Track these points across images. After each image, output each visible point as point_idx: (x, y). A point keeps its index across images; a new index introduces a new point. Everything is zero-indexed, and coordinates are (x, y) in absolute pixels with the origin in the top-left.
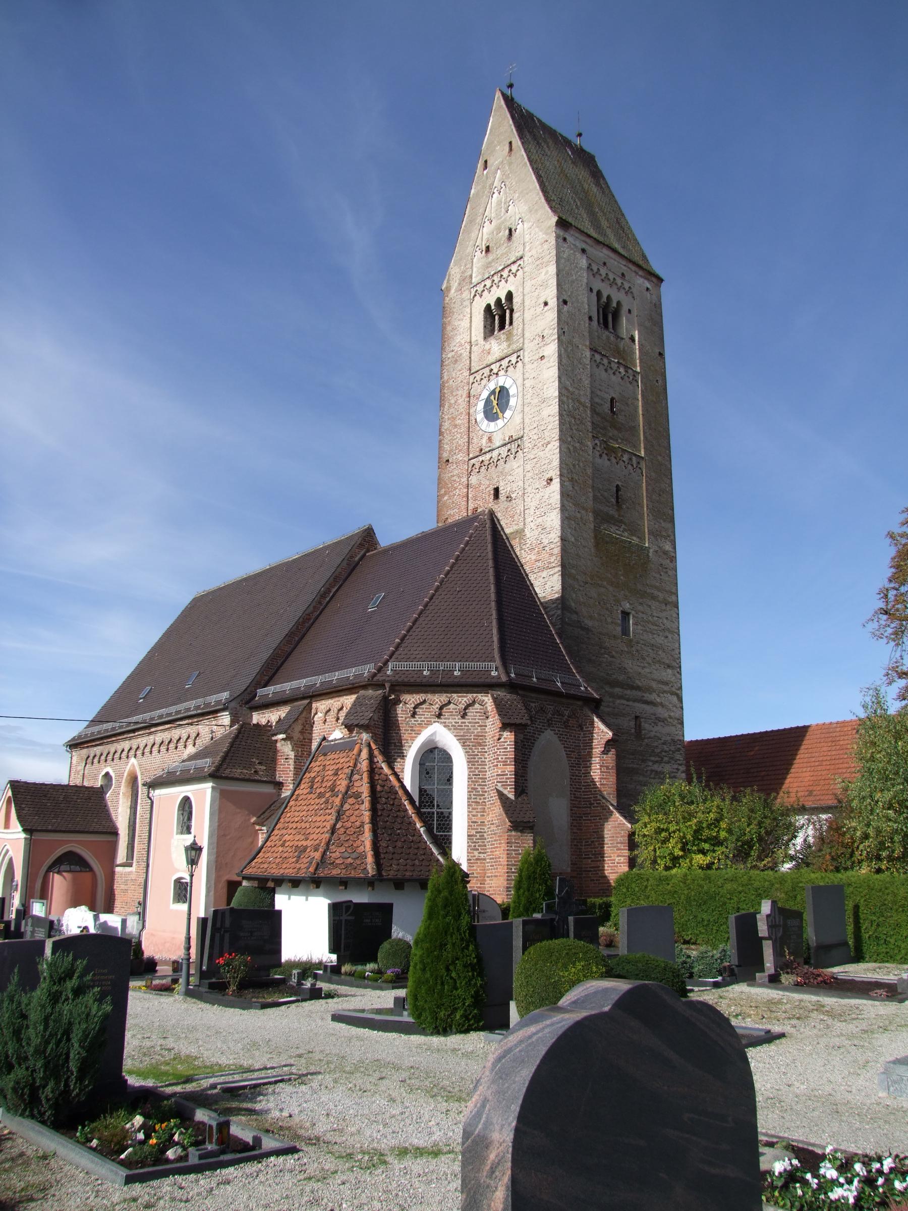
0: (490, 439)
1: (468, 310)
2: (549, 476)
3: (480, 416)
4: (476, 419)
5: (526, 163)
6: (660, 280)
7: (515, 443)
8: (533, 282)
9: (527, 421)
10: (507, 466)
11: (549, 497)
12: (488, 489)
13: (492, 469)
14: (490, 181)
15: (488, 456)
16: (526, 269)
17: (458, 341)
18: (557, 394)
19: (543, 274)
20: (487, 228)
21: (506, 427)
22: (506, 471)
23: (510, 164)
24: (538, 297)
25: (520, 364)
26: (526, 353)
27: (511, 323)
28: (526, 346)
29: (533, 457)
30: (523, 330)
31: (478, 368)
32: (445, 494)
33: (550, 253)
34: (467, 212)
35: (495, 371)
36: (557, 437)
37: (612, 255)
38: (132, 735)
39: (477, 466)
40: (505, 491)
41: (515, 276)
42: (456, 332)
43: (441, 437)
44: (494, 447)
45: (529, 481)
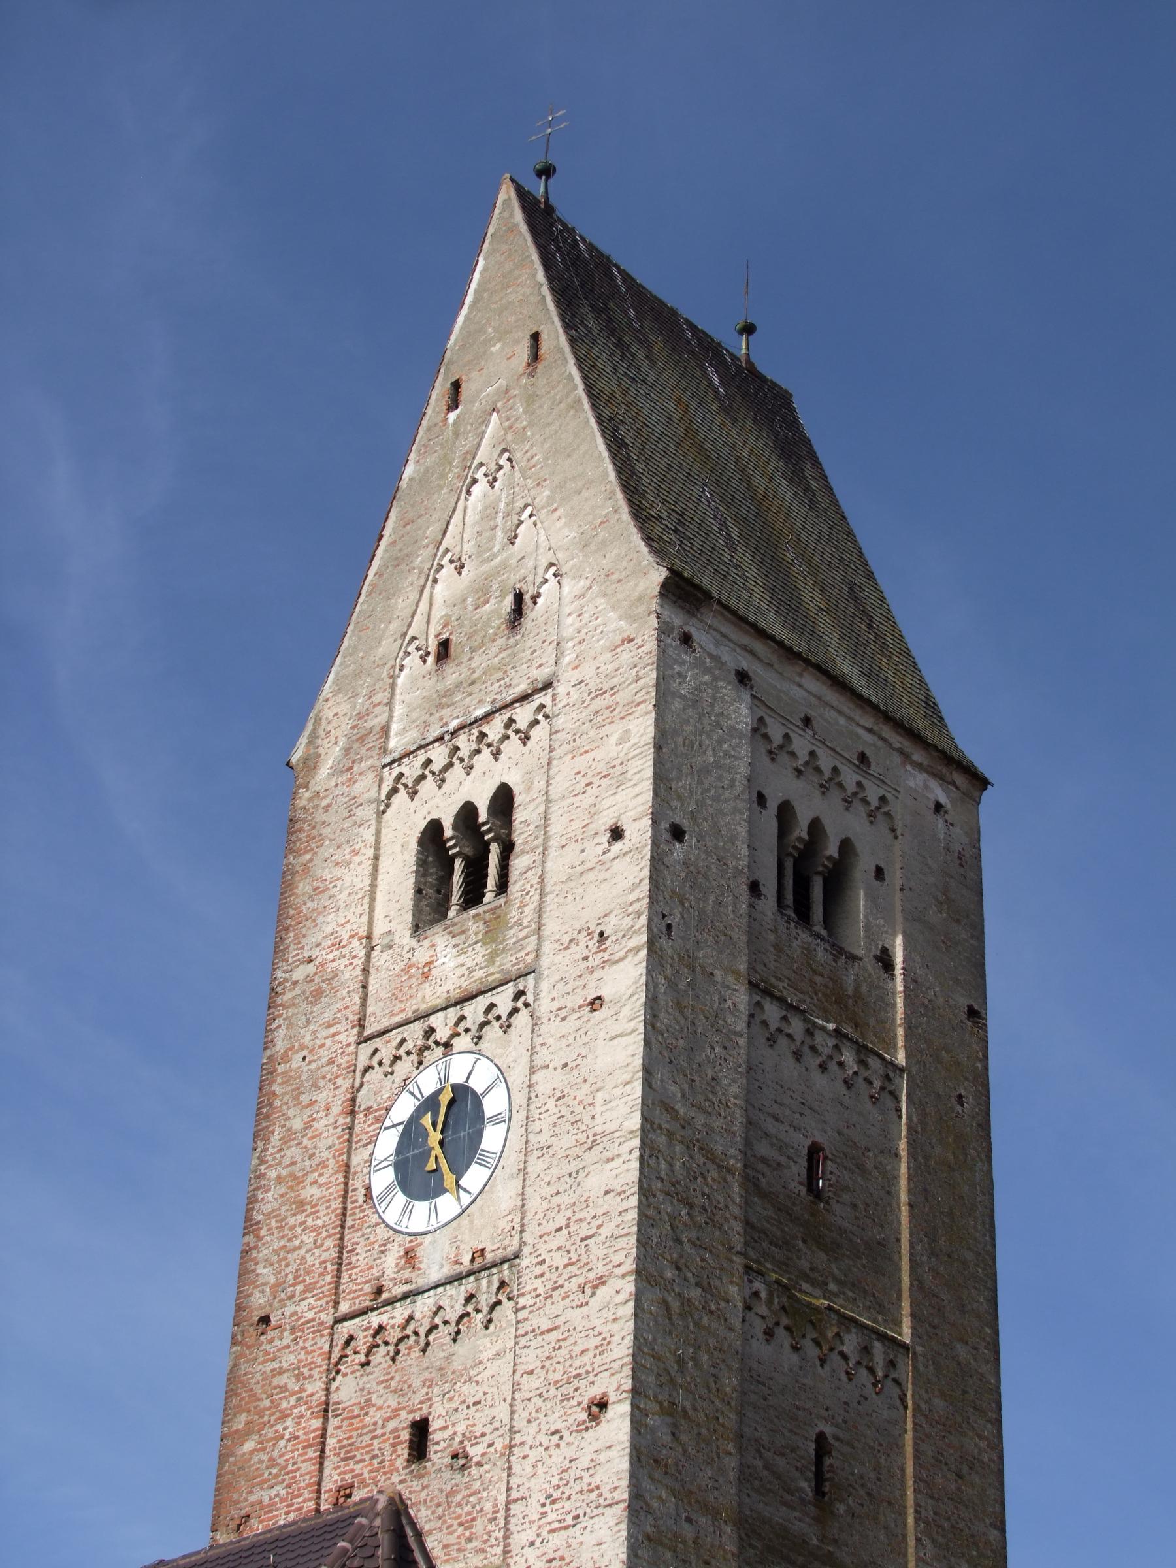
0: (410, 1257)
1: (369, 835)
2: (595, 1392)
3: (383, 1179)
4: (368, 1189)
5: (579, 400)
6: (981, 782)
8: (581, 762)
10: (462, 1349)
11: (594, 1465)
12: (392, 1425)
13: (411, 1357)
14: (464, 445)
15: (399, 1313)
16: (559, 722)
17: (328, 930)
18: (635, 1122)
19: (613, 739)
20: (448, 586)
21: (464, 1221)
22: (456, 1365)
23: (531, 399)
24: (593, 811)
25: (522, 1018)
26: (545, 986)
27: (503, 887)
28: (545, 962)
29: (546, 1324)
30: (540, 910)
31: (386, 1023)
33: (638, 679)
34: (387, 533)
35: (442, 1034)
36: (630, 1265)
37: (831, 696)
39: (362, 1344)
40: (447, 1434)
41: (525, 739)
42: (324, 900)
43: (250, 1239)
44: (421, 1282)
45: (531, 1406)
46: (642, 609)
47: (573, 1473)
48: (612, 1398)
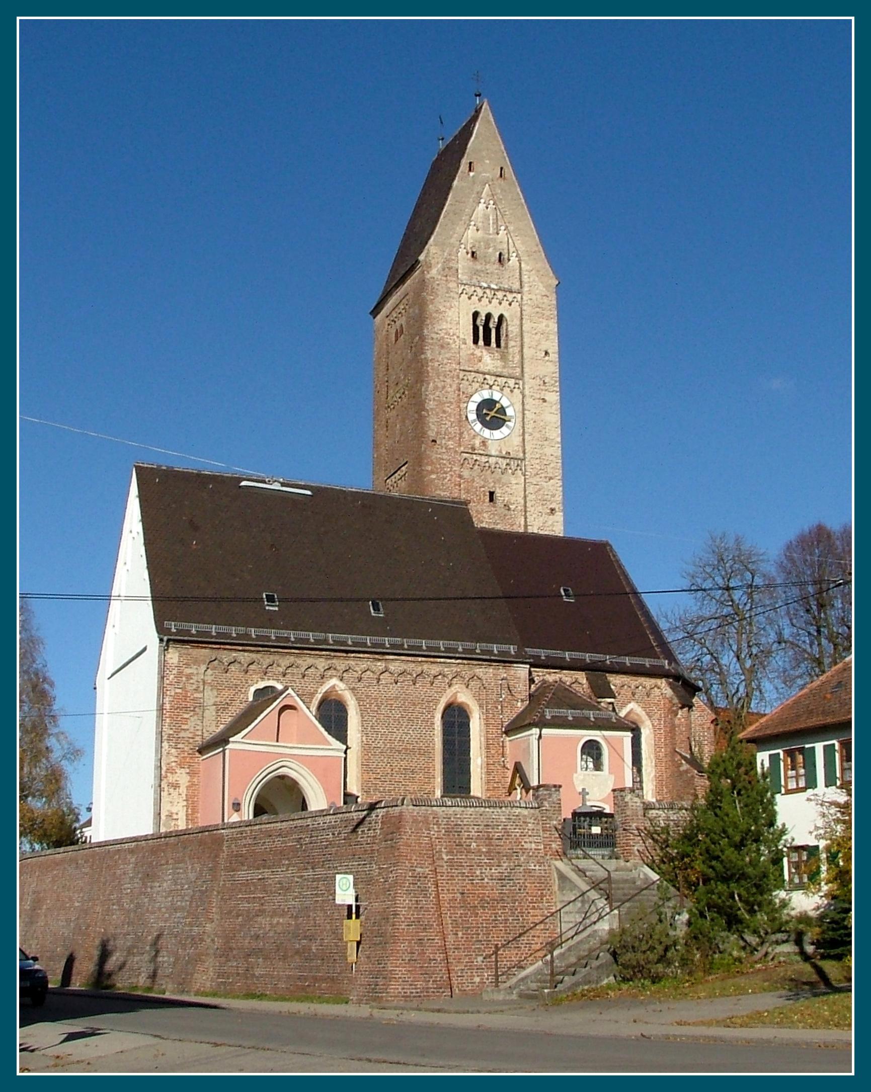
2: (552, 506)
9: (528, 448)
11: (552, 525)
15: (484, 459)
17: (444, 327)
22: (503, 481)
32: (432, 472)
38: (345, 655)
47: (546, 525)
48: (557, 510)
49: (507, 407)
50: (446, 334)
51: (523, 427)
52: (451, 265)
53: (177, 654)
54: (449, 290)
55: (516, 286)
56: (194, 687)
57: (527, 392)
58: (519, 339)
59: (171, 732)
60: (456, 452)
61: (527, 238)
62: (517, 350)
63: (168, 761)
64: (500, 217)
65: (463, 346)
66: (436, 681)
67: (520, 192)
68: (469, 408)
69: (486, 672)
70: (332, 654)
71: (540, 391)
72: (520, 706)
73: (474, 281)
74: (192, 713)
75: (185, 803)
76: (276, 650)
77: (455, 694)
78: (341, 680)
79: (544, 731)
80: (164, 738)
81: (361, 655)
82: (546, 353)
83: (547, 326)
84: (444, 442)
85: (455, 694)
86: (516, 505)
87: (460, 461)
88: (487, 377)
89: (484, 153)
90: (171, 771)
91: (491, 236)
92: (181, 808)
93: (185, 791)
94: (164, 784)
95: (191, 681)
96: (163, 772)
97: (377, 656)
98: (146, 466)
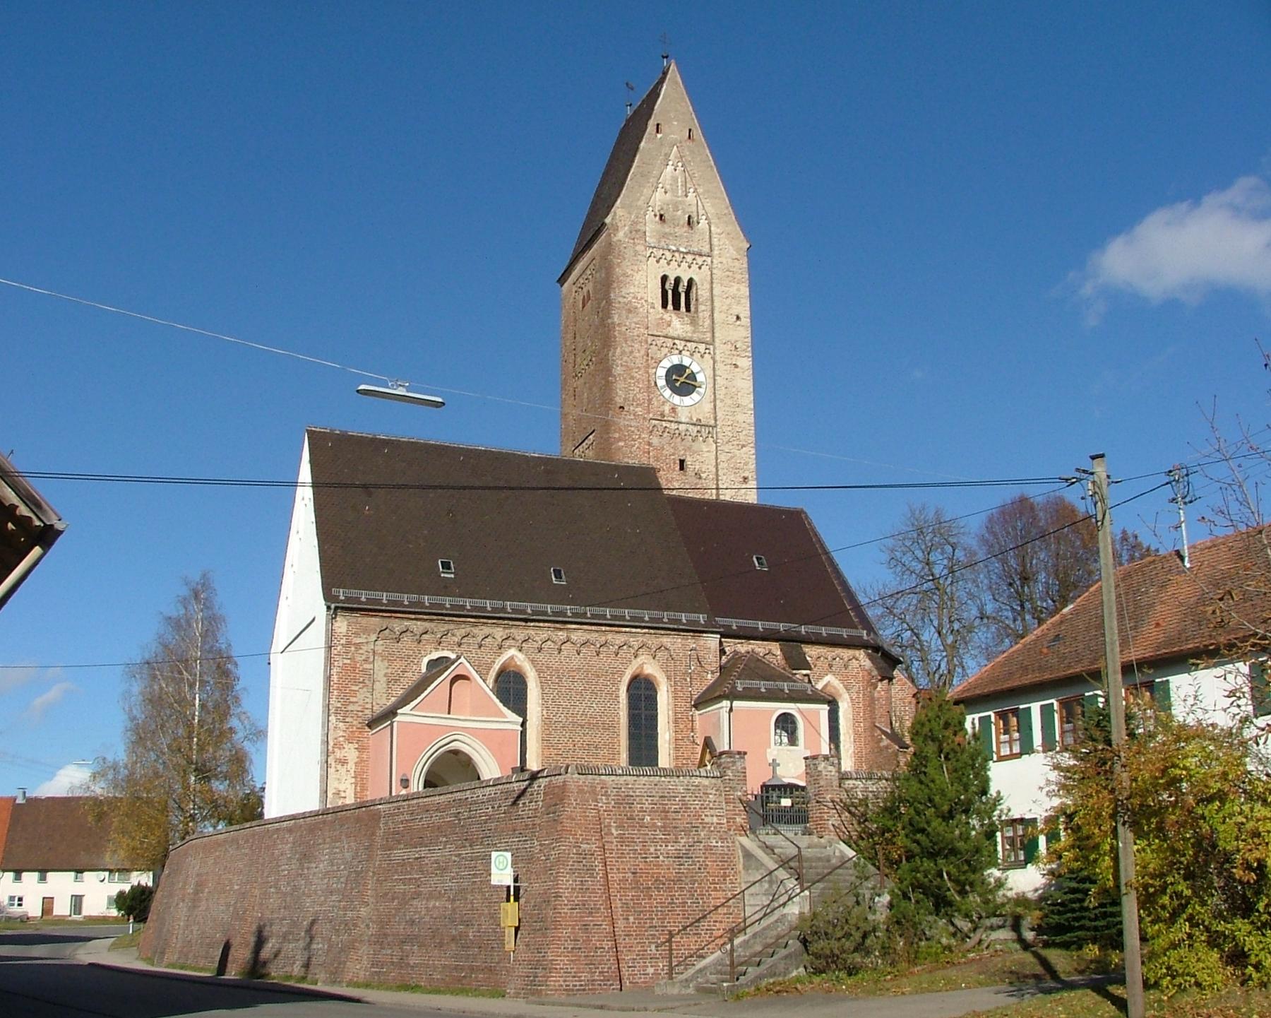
2: (746, 474)
7: (705, 428)
8: (724, 288)
9: (719, 414)
15: (674, 426)
32: (620, 440)
38: (524, 624)
46: (741, 252)
48: (750, 478)
49: (697, 373)
50: (634, 298)
51: (715, 393)
52: (638, 227)
53: (346, 623)
54: (636, 253)
55: (706, 249)
56: (364, 657)
57: (718, 358)
58: (709, 303)
59: (339, 705)
60: (644, 418)
61: (717, 201)
62: (707, 314)
63: (336, 736)
64: (688, 179)
65: (651, 310)
66: (621, 652)
67: (709, 155)
68: (658, 374)
69: (673, 642)
70: (511, 623)
71: (731, 357)
72: (710, 678)
73: (663, 244)
74: (361, 685)
75: (353, 780)
76: (451, 618)
77: (641, 666)
78: (520, 650)
79: (736, 703)
80: (331, 712)
81: (541, 624)
82: (738, 318)
83: (738, 290)
84: (632, 408)
85: (641, 666)
86: (706, 474)
87: (649, 428)
88: (676, 341)
89: (672, 115)
90: (338, 746)
91: (680, 199)
92: (349, 786)
93: (354, 767)
94: (331, 760)
95: (361, 651)
96: (330, 748)
97: (558, 626)
98: (318, 430)
